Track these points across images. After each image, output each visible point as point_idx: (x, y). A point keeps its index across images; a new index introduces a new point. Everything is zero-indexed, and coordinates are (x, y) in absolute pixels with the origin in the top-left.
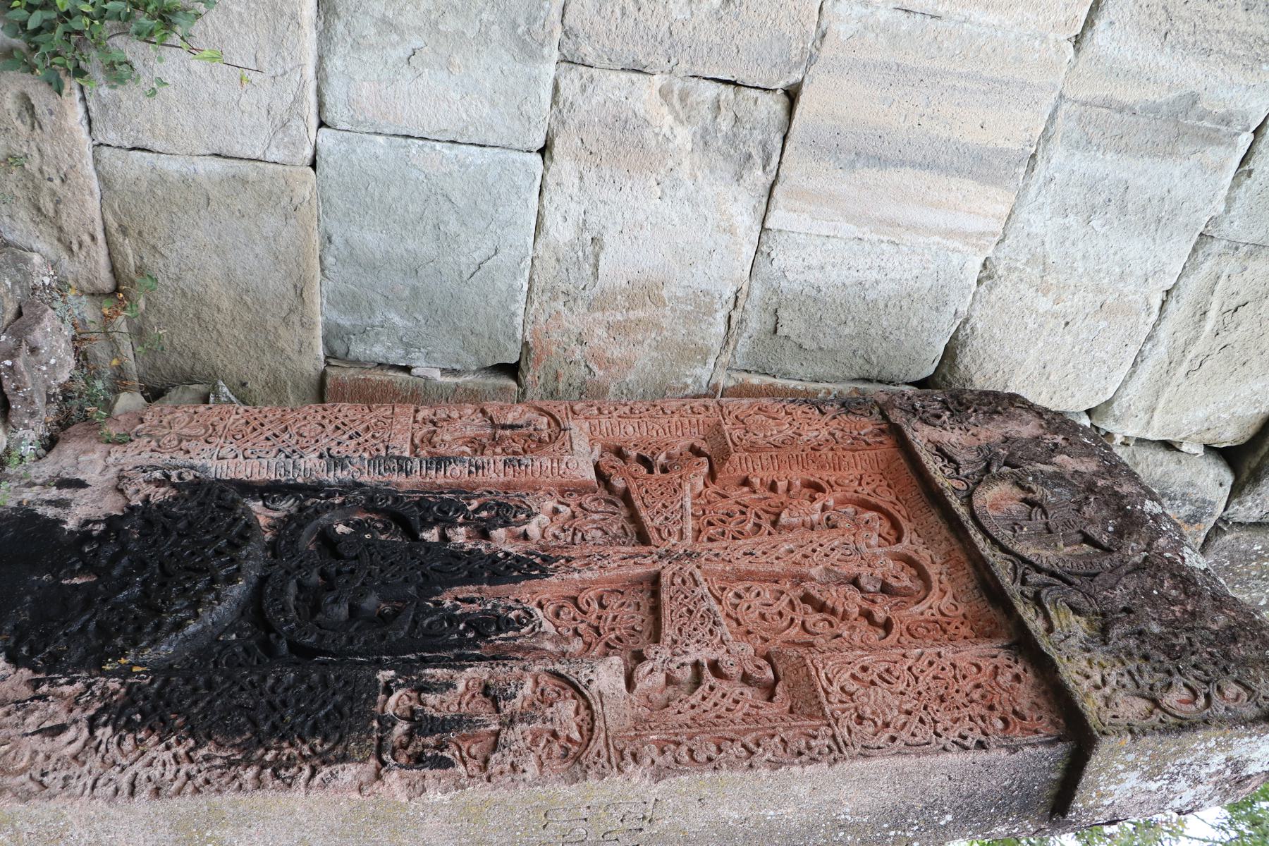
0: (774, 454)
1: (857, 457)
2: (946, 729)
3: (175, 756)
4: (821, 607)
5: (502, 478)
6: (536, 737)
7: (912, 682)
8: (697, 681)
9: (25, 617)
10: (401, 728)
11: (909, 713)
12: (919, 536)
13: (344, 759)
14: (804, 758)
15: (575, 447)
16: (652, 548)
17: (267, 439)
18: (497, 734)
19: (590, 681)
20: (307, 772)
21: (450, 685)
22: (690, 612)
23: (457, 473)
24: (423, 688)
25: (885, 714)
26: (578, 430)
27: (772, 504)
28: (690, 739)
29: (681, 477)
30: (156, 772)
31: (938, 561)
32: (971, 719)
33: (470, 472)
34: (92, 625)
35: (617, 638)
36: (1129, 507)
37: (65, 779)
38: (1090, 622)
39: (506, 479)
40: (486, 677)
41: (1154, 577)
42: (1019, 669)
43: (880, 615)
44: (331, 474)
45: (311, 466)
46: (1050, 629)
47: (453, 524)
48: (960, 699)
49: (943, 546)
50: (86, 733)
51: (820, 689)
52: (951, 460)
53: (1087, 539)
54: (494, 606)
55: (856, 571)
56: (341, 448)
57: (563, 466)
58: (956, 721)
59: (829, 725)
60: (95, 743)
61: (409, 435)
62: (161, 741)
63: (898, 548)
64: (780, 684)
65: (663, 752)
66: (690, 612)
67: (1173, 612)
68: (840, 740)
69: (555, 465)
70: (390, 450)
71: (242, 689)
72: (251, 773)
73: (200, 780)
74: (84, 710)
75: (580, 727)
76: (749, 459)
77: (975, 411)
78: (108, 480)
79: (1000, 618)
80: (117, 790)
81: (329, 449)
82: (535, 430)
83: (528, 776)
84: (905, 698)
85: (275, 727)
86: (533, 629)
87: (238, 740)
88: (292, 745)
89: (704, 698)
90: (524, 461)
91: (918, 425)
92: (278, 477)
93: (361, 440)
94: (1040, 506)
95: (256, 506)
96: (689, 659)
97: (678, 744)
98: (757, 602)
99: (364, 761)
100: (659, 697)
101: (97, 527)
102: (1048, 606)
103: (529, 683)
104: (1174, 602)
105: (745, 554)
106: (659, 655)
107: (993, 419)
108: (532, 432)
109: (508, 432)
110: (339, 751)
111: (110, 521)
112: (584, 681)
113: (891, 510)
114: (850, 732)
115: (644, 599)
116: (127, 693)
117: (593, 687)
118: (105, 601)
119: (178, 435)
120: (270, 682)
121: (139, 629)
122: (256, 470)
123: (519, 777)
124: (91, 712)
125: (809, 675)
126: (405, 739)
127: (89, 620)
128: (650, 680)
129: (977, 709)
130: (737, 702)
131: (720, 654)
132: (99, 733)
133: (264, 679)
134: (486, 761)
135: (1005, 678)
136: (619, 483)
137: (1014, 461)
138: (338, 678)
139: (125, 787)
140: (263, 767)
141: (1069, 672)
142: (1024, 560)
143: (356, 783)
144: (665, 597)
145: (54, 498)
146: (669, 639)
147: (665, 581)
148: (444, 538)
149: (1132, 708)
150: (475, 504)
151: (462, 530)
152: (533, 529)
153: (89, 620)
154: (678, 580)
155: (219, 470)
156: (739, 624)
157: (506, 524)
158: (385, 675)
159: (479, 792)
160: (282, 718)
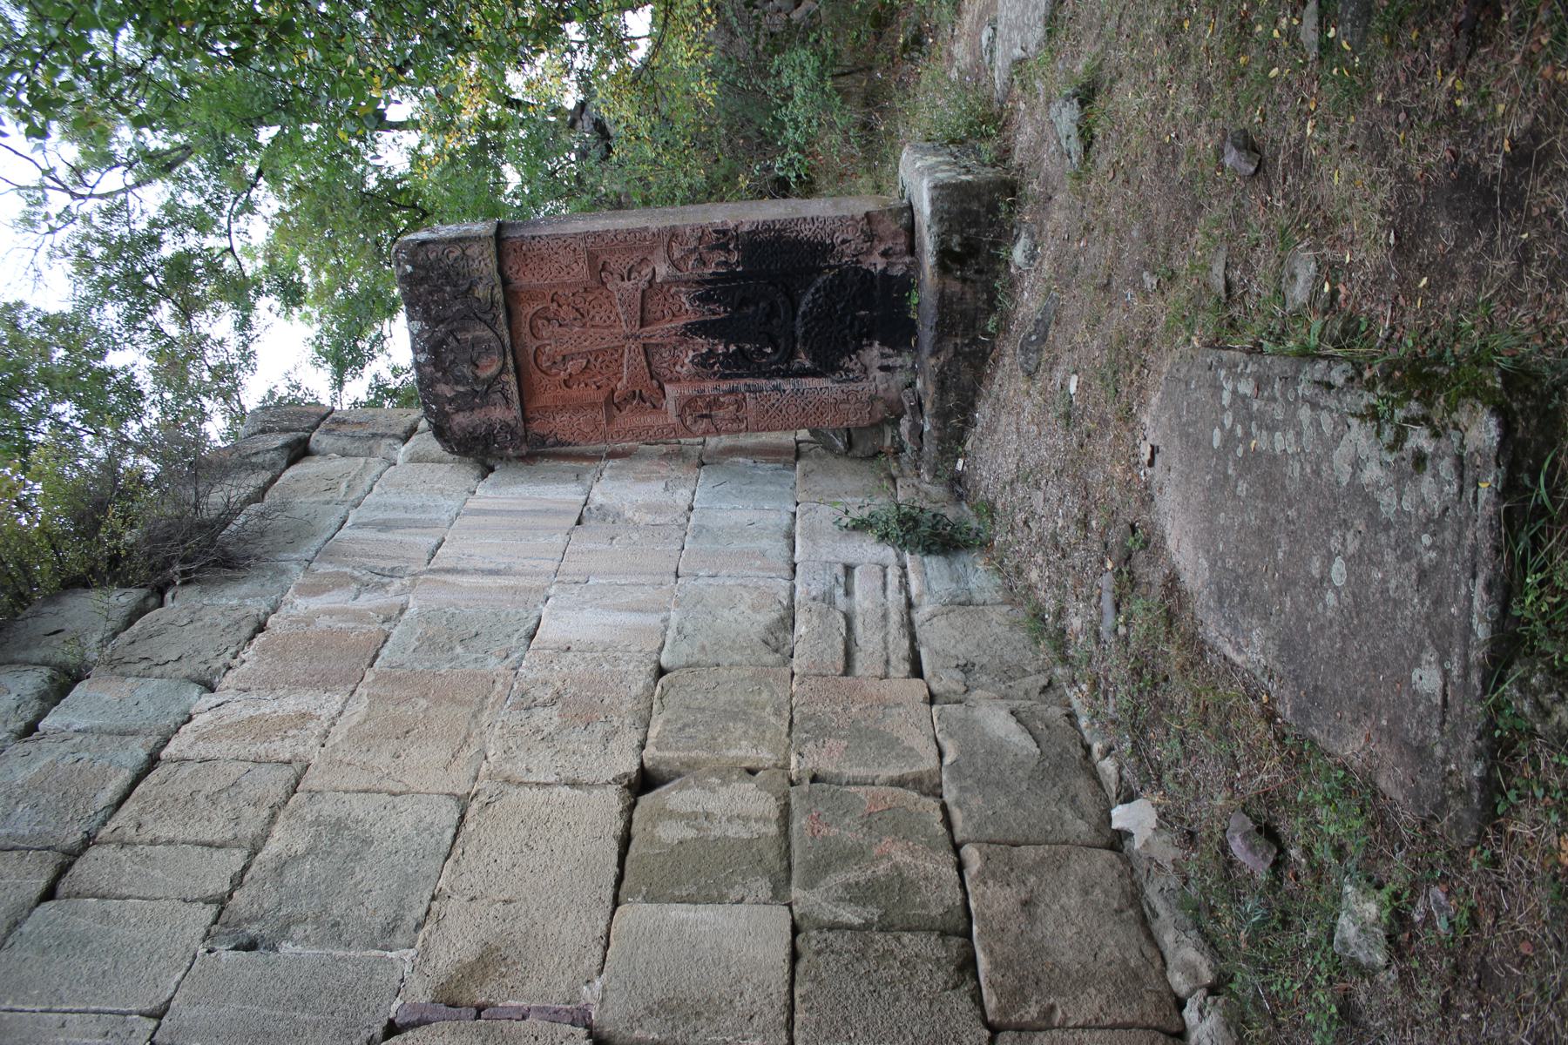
4: (577, 310)
8: (630, 272)
9: (875, 294)
10: (731, 246)
13: (748, 233)
21: (717, 265)
23: (725, 386)
24: (726, 263)
26: (673, 418)
43: (555, 304)
45: (788, 385)
48: (535, 259)
53: (458, 340)
55: (560, 330)
63: (538, 343)
91: (513, 423)
95: (808, 364)
100: (643, 266)
106: (643, 285)
111: (862, 347)
115: (649, 317)
128: (647, 271)
129: (530, 254)
131: (621, 284)
135: (515, 268)
136: (654, 382)
141: (493, 265)
147: (638, 323)
148: (727, 347)
149: (474, 250)
152: (691, 354)
157: (702, 355)
158: (740, 269)
159: (705, 222)
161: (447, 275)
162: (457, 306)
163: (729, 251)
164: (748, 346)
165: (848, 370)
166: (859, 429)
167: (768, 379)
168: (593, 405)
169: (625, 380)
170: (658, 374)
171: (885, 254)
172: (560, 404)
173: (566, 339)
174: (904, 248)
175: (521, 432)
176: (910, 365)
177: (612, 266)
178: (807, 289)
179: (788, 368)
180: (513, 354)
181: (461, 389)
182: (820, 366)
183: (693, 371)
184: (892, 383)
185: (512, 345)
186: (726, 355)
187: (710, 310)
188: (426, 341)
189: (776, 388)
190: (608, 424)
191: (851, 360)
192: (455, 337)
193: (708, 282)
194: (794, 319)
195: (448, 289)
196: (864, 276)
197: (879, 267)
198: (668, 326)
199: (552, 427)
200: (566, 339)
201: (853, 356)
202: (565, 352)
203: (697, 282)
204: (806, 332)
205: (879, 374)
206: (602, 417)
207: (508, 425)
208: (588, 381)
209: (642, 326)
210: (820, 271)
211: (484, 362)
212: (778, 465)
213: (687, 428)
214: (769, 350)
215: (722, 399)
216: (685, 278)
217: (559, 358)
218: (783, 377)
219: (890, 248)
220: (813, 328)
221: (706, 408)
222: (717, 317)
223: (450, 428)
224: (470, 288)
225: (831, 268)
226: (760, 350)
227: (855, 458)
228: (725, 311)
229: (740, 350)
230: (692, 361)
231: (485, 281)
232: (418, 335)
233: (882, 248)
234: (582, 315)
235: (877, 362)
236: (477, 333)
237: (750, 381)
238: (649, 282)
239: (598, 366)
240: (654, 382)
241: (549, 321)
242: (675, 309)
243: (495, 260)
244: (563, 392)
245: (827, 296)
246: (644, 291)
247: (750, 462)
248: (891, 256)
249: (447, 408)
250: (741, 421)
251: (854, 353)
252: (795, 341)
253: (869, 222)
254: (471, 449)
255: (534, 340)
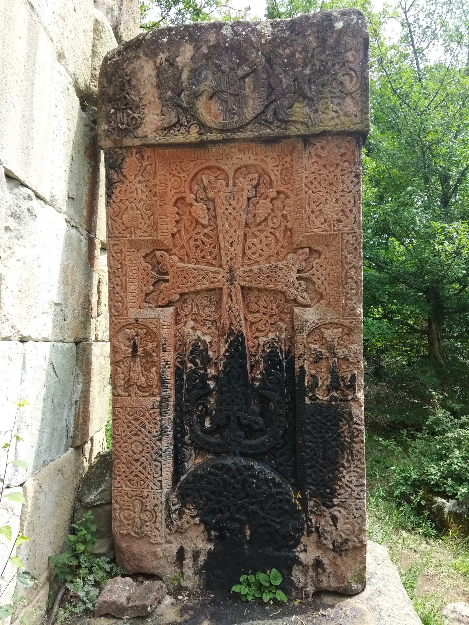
0: (159, 217)
1: (161, 173)
2: (347, 188)
3: (347, 474)
4: (266, 219)
5: (172, 352)
6: (339, 344)
7: (322, 194)
10: (334, 393)
11: (337, 200)
12: (222, 159)
13: (350, 414)
14: (358, 247)
15: (153, 316)
16: (225, 287)
17: (145, 468)
18: (338, 358)
19: (313, 323)
20: (356, 426)
21: (314, 376)
22: (268, 277)
24: (315, 385)
25: (338, 210)
27: (190, 224)
28: (345, 288)
29: (172, 267)
30: (354, 479)
31: (241, 156)
32: (343, 175)
33: (169, 368)
34: (278, 520)
35: (277, 308)
36: (227, 45)
37: (357, 509)
38: (298, 102)
39: (172, 351)
40: (308, 362)
41: (276, 57)
42: (319, 145)
43: (274, 195)
44: (169, 433)
46: (302, 123)
47: (205, 375)
49: (233, 150)
50: (335, 508)
51: (324, 233)
52: (174, 125)
53: (243, 78)
54: (262, 357)
55: (246, 198)
56: (154, 430)
57: (166, 323)
58: (343, 183)
59: (342, 234)
60: (341, 503)
61: (142, 399)
62: (341, 480)
63: (231, 173)
64: (313, 247)
65: (351, 299)
66: (268, 277)
67: (299, 58)
68: (350, 232)
69: (165, 327)
70: (156, 407)
71: (315, 454)
72: (355, 445)
73: (358, 463)
74: (325, 511)
75: (337, 328)
76: (162, 230)
77: (128, 94)
78: (176, 539)
79: (288, 141)
80: (362, 491)
81: (154, 436)
82: (137, 335)
83: (358, 348)
84: (329, 199)
85: (335, 440)
86: (275, 342)
87: (340, 452)
88: (343, 432)
89: (318, 279)
90: (164, 342)
91: (140, 132)
92: (171, 458)
93: (146, 422)
94: (217, 92)
96: (297, 283)
97: (347, 293)
98: (260, 246)
99: (351, 406)
101: (213, 534)
102: (290, 119)
103: (312, 346)
104: (293, 54)
105: (231, 246)
106: (292, 292)
107: (135, 86)
108: (139, 337)
109: (140, 350)
110: (346, 415)
111: (208, 529)
112: (313, 325)
113: (201, 167)
114: (345, 226)
116: (315, 497)
117: (317, 322)
118: (263, 518)
119: (141, 512)
120: (310, 444)
121: (281, 501)
122: (168, 469)
123: (358, 351)
124: (325, 508)
125: (314, 236)
126: (339, 392)
127: (275, 522)
129: (338, 171)
130: (321, 266)
131: (295, 269)
132: (336, 503)
133: (309, 447)
134: (351, 363)
137: (178, 91)
138: (308, 418)
139: (360, 488)
140: (354, 442)
142: (256, 117)
143: (359, 408)
144: (259, 286)
145: (192, 559)
146: (284, 288)
147: (248, 285)
150: (189, 365)
151: (209, 371)
152: (207, 339)
153: (275, 522)
154: (248, 279)
155: (168, 487)
156: (272, 256)
160: (329, 437)
161: (324, 71)
162: (286, 82)
163: (329, 390)
164: (212, 401)
165: (181, 513)
166: (109, 518)
167: (174, 421)
168: (155, 227)
169: (182, 264)
170: (185, 302)
171: (318, 564)
172: (158, 189)
173: (234, 204)
174: (324, 585)
175: (128, 142)
176: (185, 583)
177: (316, 262)
178: (276, 470)
179: (184, 443)
180: (224, 141)
181: (185, 75)
182: (187, 481)
183: (188, 340)
184: (163, 562)
185: (234, 140)
186: (205, 377)
187: (258, 362)
188: (247, 39)
189: (163, 431)
190: (130, 241)
191: (193, 517)
192: (248, 75)
193: (291, 363)
194: (243, 454)
195: (307, 72)
196: (293, 538)
197: (302, 556)
198: (242, 317)
199: (131, 178)
200: (234, 204)
201: (197, 520)
202: (218, 201)
203: (290, 352)
204: (229, 468)
205: (174, 548)
206: (139, 235)
207: (137, 127)
208: (182, 224)
209: (242, 288)
210: (298, 487)
211: (215, 106)
212: (72, 430)
213: (121, 329)
214: (207, 424)
215: (154, 370)
216: (298, 339)
217: (211, 195)
218: (175, 438)
219: (324, 570)
220: (233, 477)
221: (145, 352)
222: (249, 371)
223: (137, 57)
224: (305, 97)
225: (304, 502)
226: (208, 413)
227: (74, 511)
228: (254, 379)
229: (209, 393)
230: (199, 339)
231: (312, 116)
232: (254, 30)
233: (325, 561)
234: (260, 224)
235: (189, 547)
236: (251, 102)
237: (172, 401)
238: (295, 300)
239: (198, 237)
240: (177, 297)
241: (255, 187)
242: (260, 325)
243: (339, 128)
244: (171, 197)
245: (271, 495)
246: (283, 293)
247: (77, 396)
248: (315, 570)
249: (162, 56)
250: (126, 390)
251: (201, 521)
252: (217, 454)
253: (355, 548)
254: (109, 81)
255: (235, 167)
